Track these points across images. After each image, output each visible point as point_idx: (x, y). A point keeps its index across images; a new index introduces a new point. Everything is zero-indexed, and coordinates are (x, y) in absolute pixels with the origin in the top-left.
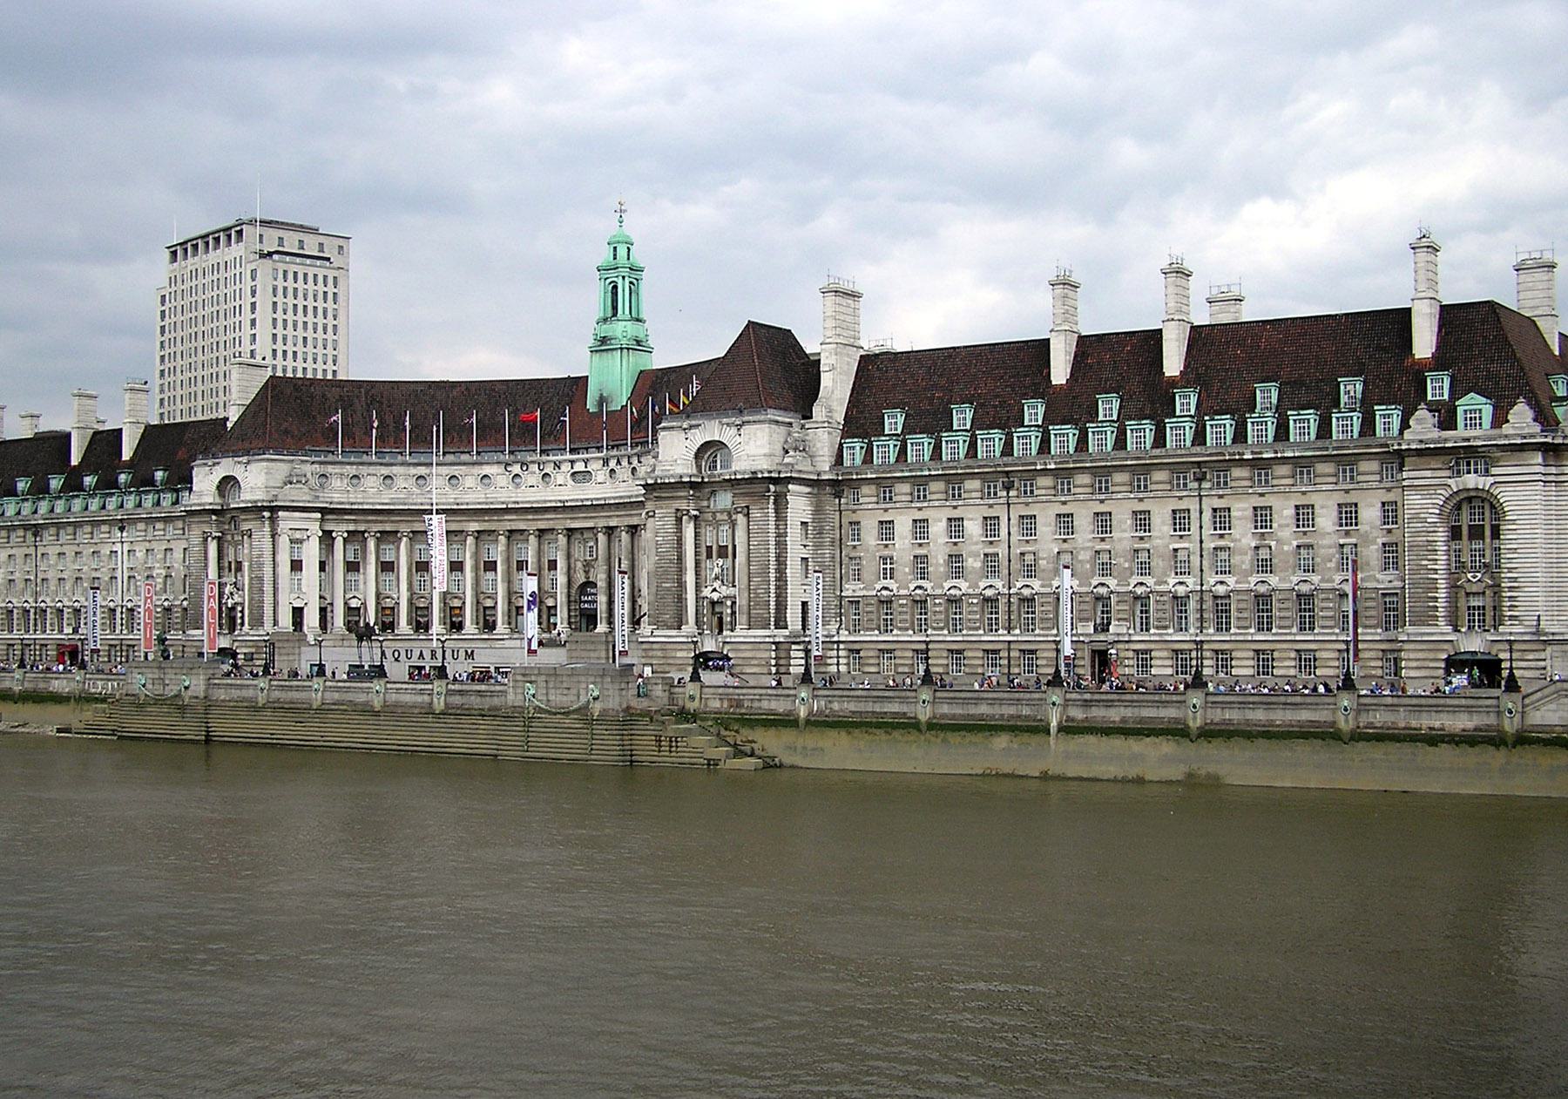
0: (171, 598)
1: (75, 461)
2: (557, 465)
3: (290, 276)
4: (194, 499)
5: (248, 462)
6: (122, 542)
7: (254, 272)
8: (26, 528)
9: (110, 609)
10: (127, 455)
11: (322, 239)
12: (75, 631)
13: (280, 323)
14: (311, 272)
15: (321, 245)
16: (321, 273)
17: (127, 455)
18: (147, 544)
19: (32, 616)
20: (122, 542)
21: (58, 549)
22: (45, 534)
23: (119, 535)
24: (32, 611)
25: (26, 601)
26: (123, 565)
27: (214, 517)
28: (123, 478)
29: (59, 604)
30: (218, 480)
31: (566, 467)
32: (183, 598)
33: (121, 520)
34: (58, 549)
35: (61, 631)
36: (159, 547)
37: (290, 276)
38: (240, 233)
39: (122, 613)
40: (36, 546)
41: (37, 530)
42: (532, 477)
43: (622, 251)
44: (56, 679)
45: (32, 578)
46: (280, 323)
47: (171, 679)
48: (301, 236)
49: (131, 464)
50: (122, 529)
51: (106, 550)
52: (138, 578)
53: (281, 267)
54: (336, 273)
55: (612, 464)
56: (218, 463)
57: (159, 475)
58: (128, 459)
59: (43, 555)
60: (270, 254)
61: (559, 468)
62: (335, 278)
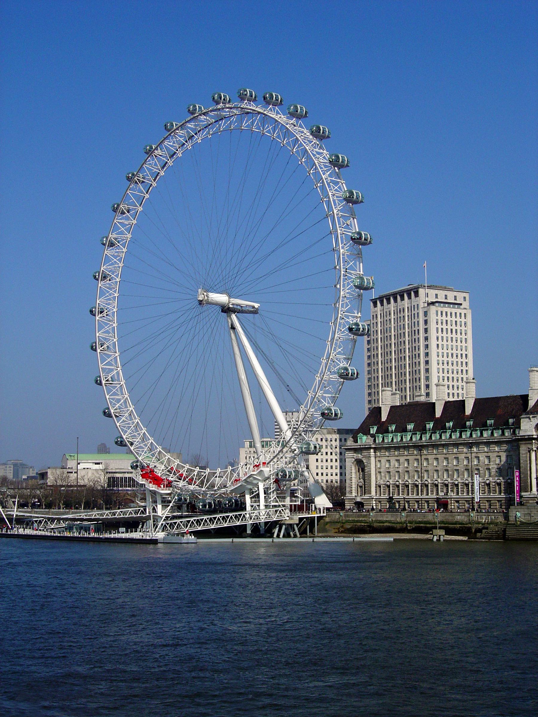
1: (438, 413)
3: (444, 314)
4: (522, 433)
6: (471, 453)
7: (426, 314)
9: (486, 484)
10: (468, 410)
11: (455, 294)
12: (447, 494)
13: (440, 339)
14: (454, 311)
15: (455, 297)
16: (458, 311)
17: (468, 410)
20: (471, 453)
21: (434, 456)
25: (417, 481)
27: (534, 441)
28: (468, 423)
29: (436, 482)
30: (535, 424)
32: (507, 478)
34: (434, 456)
35: (437, 494)
37: (444, 314)
38: (417, 294)
40: (421, 455)
44: (458, 515)
45: (419, 470)
46: (440, 339)
47: (534, 514)
48: (446, 292)
49: (471, 417)
50: (471, 448)
52: (480, 469)
53: (440, 309)
54: (465, 311)
56: (535, 417)
57: (489, 422)
58: (469, 414)
60: (433, 303)
62: (465, 314)
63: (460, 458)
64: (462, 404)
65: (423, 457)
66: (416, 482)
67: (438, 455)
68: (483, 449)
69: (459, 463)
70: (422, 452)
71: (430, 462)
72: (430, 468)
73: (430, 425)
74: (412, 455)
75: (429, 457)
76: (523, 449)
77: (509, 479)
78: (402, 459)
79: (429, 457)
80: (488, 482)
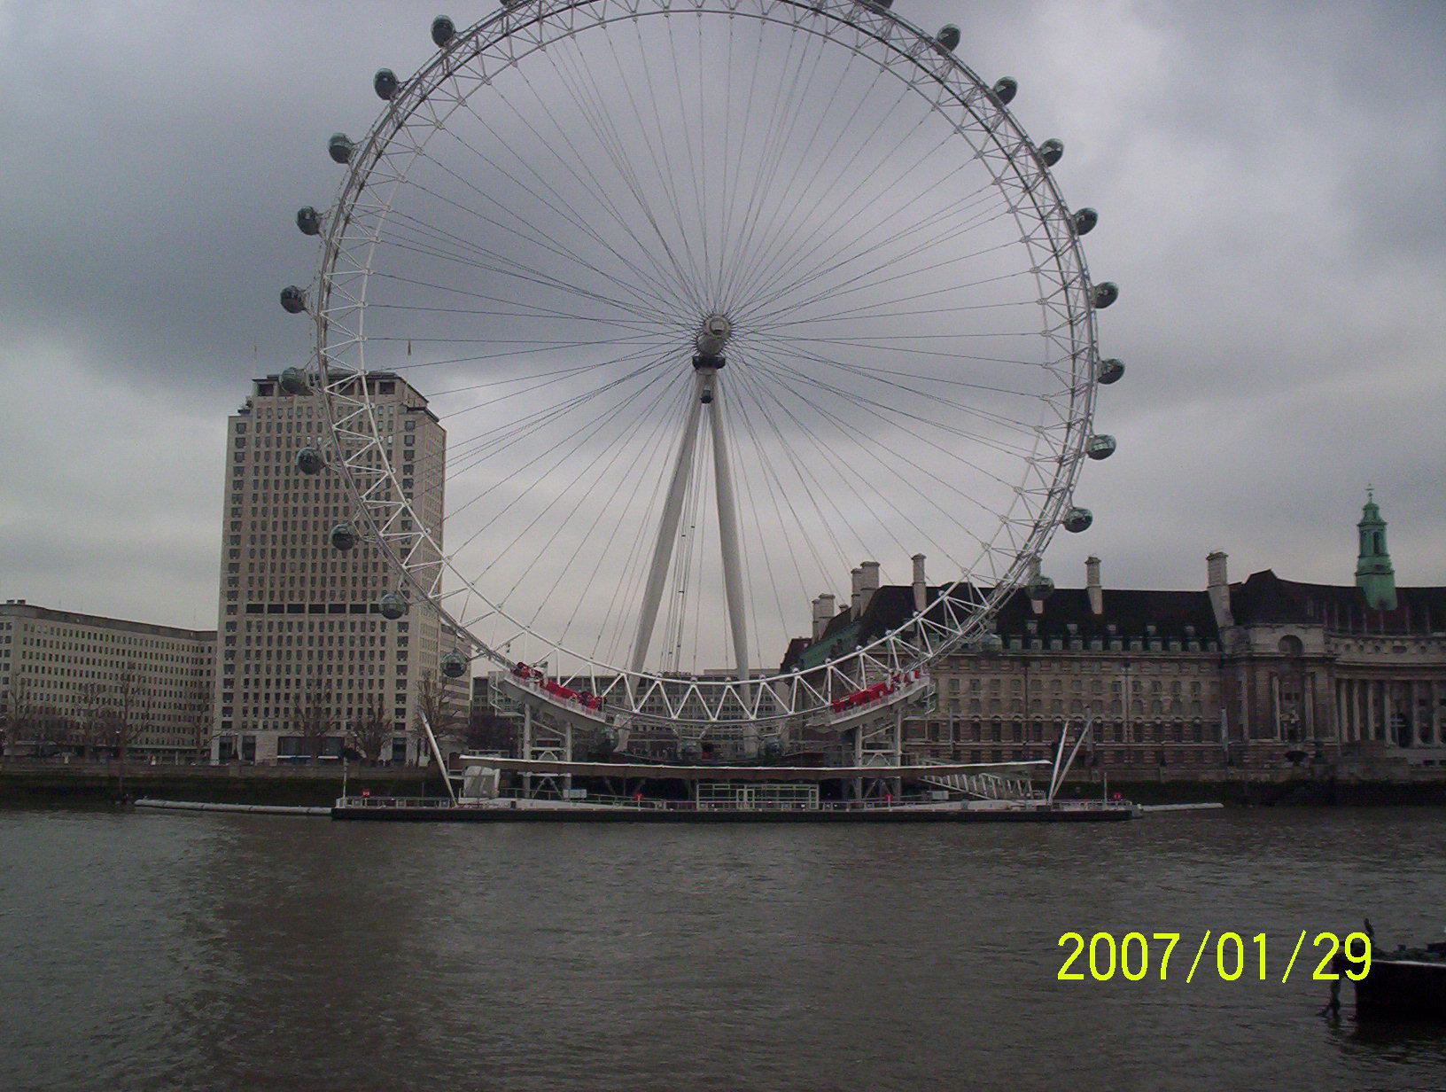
0: (1181, 716)
2: (1383, 641)
5: (1310, 628)
8: (1012, 659)
10: (1097, 608)
17: (1097, 608)
18: (1154, 678)
19: (1024, 729)
20: (1126, 676)
21: (1052, 677)
22: (1034, 665)
23: (1124, 669)
24: (1024, 724)
26: (1126, 694)
31: (1388, 643)
34: (1052, 677)
36: (1166, 683)
39: (1128, 727)
41: (1026, 662)
42: (1369, 648)
43: (1375, 514)
50: (1127, 666)
51: (1108, 680)
55: (1423, 644)
61: (1384, 643)
63: (1103, 681)
64: (1081, 596)
65: (1030, 678)
66: (1017, 719)
72: (1044, 696)
73: (1032, 626)
75: (1043, 678)
76: (1262, 675)
77: (1198, 718)
78: (985, 679)
79: (1043, 678)
80: (1158, 722)
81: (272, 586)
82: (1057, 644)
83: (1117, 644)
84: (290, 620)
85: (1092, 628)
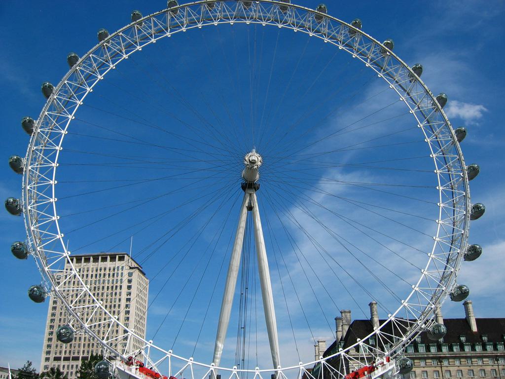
6: (498, 366)
7: (130, 275)
10: (475, 328)
17: (475, 328)
21: (456, 368)
22: (445, 363)
33: (497, 356)
34: (456, 368)
41: (440, 359)
50: (497, 360)
59: (446, 371)
65: (444, 369)
67: (449, 367)
68: (487, 362)
69: (486, 375)
70: (442, 363)
71: (452, 374)
74: (430, 366)
79: (451, 369)
81: (66, 348)
82: (456, 349)
83: (490, 348)
84: (72, 364)
85: (474, 340)
